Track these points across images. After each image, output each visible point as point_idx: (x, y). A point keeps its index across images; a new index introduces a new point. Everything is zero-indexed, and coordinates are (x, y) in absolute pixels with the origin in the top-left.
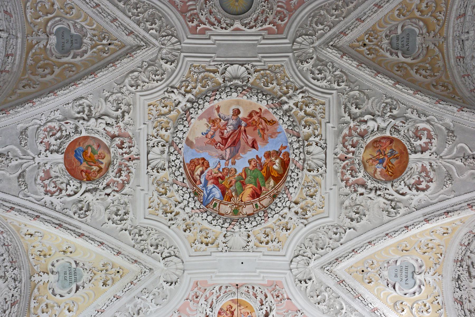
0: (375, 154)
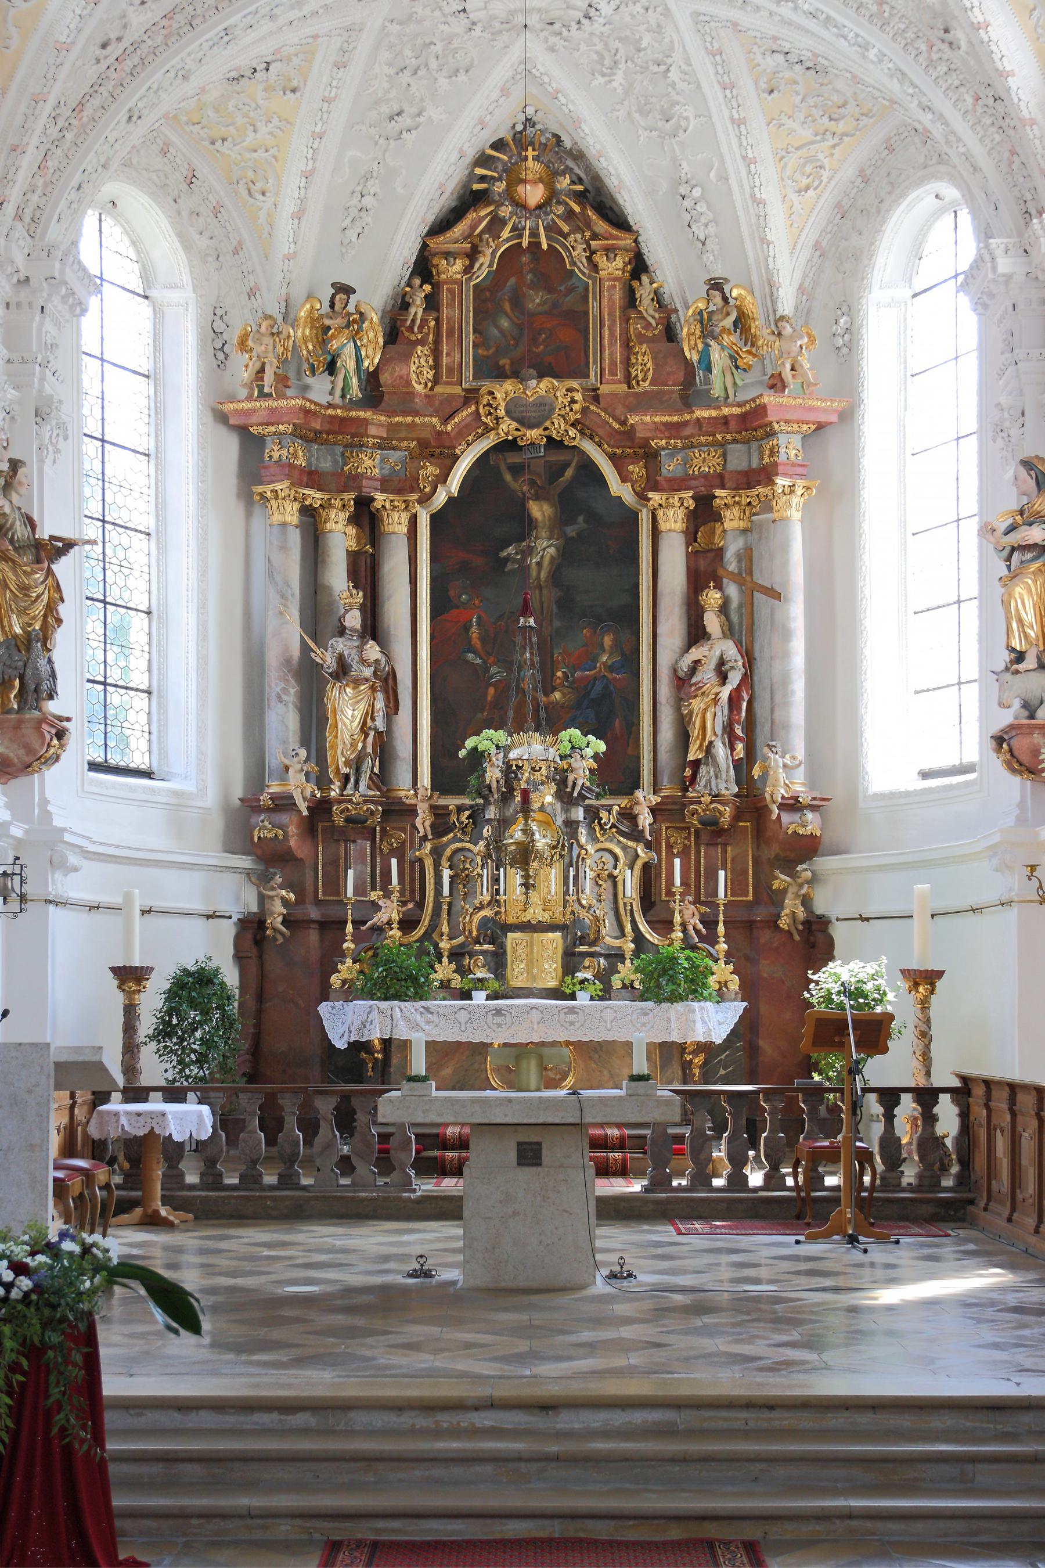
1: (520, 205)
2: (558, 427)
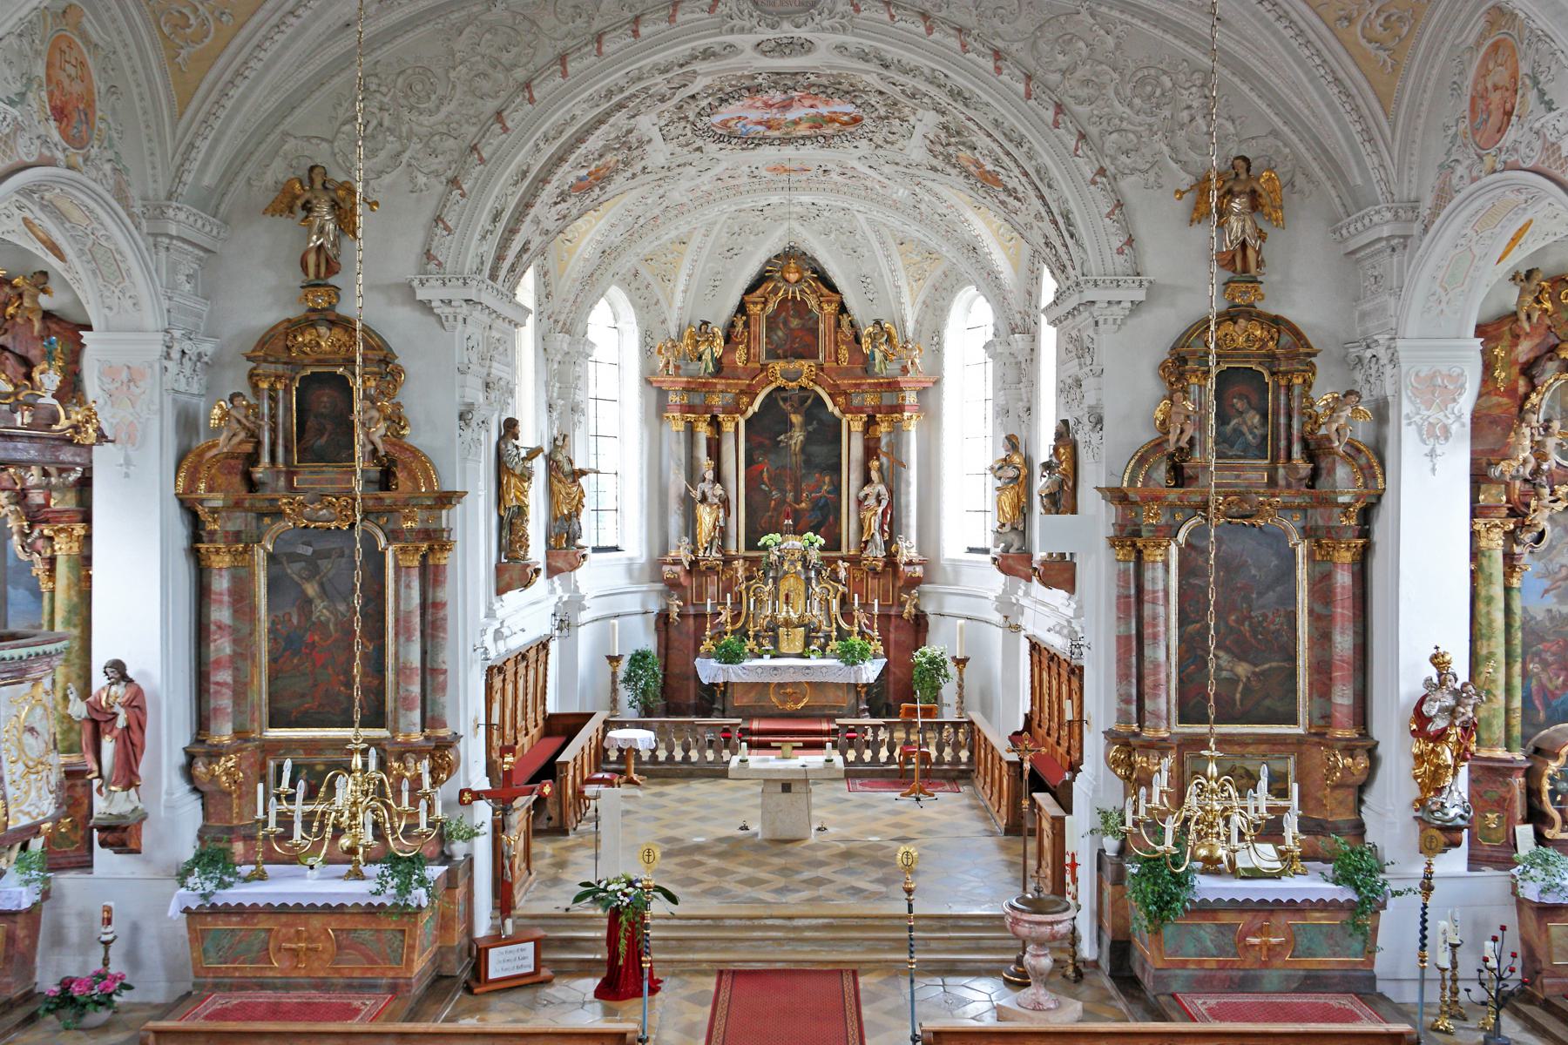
2: (804, 381)
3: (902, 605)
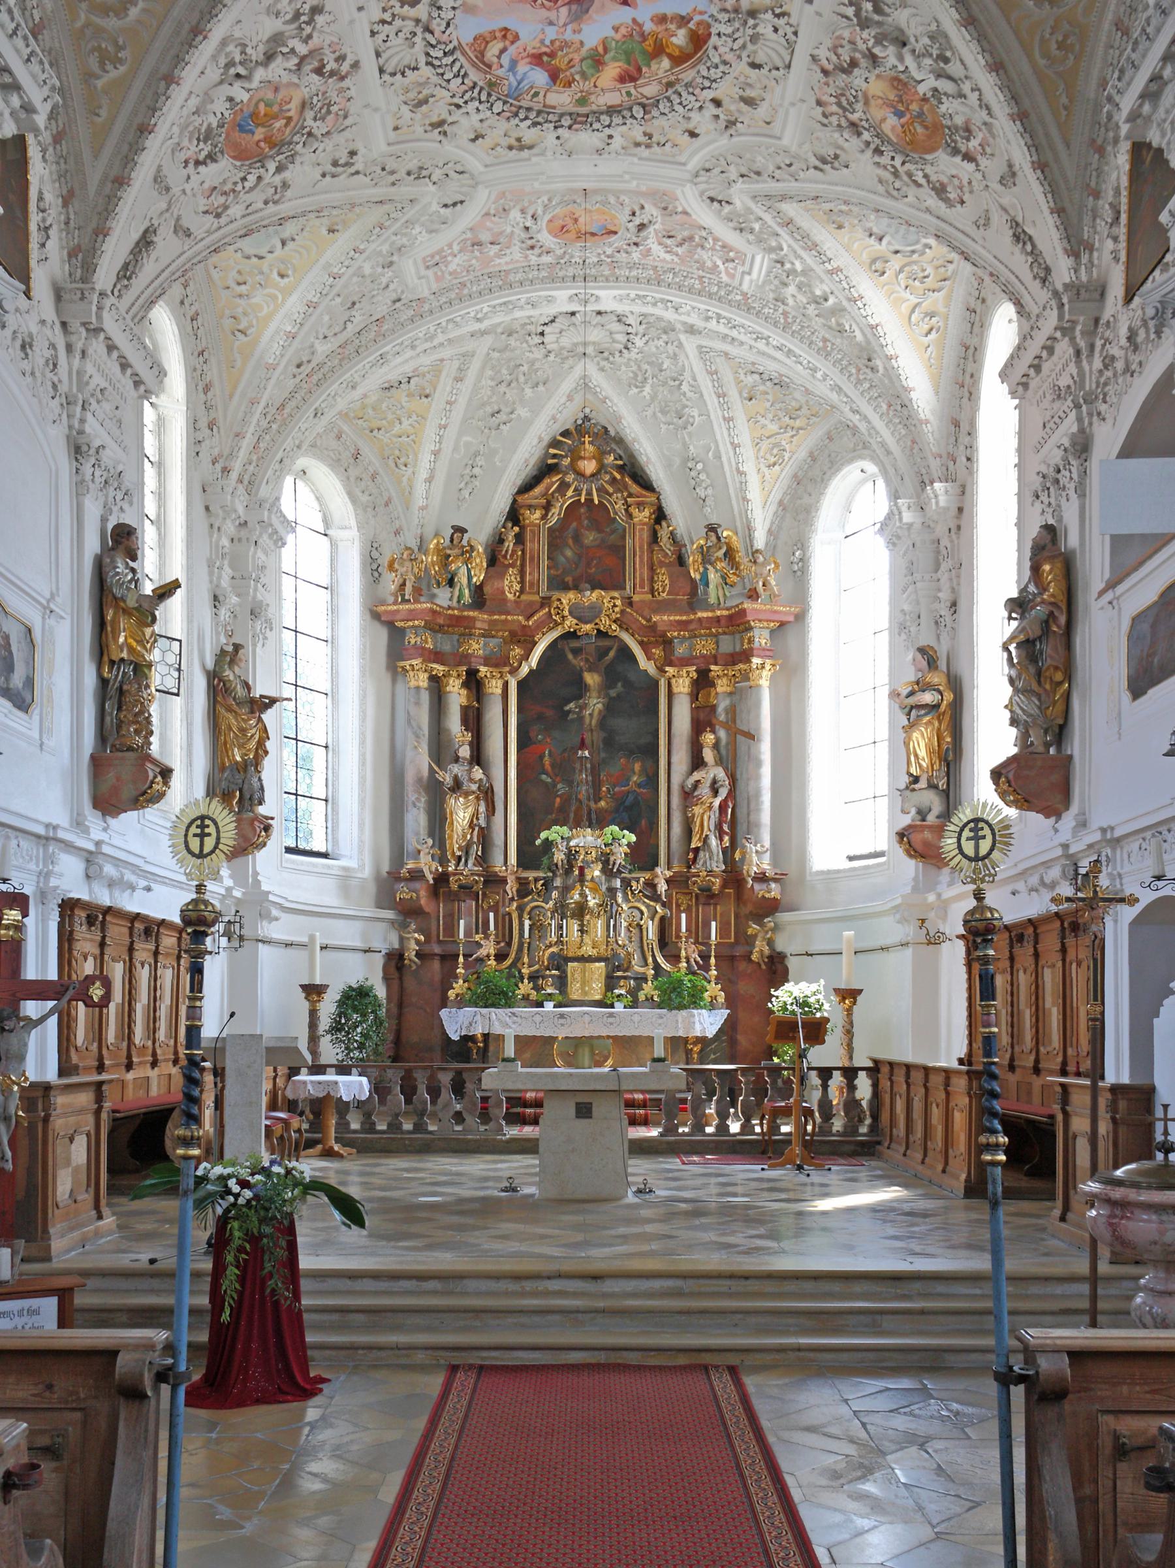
0: (892, 97)
1: (580, 474)
2: (604, 623)
3: (750, 941)
